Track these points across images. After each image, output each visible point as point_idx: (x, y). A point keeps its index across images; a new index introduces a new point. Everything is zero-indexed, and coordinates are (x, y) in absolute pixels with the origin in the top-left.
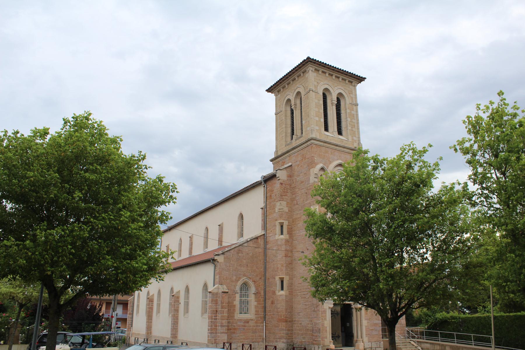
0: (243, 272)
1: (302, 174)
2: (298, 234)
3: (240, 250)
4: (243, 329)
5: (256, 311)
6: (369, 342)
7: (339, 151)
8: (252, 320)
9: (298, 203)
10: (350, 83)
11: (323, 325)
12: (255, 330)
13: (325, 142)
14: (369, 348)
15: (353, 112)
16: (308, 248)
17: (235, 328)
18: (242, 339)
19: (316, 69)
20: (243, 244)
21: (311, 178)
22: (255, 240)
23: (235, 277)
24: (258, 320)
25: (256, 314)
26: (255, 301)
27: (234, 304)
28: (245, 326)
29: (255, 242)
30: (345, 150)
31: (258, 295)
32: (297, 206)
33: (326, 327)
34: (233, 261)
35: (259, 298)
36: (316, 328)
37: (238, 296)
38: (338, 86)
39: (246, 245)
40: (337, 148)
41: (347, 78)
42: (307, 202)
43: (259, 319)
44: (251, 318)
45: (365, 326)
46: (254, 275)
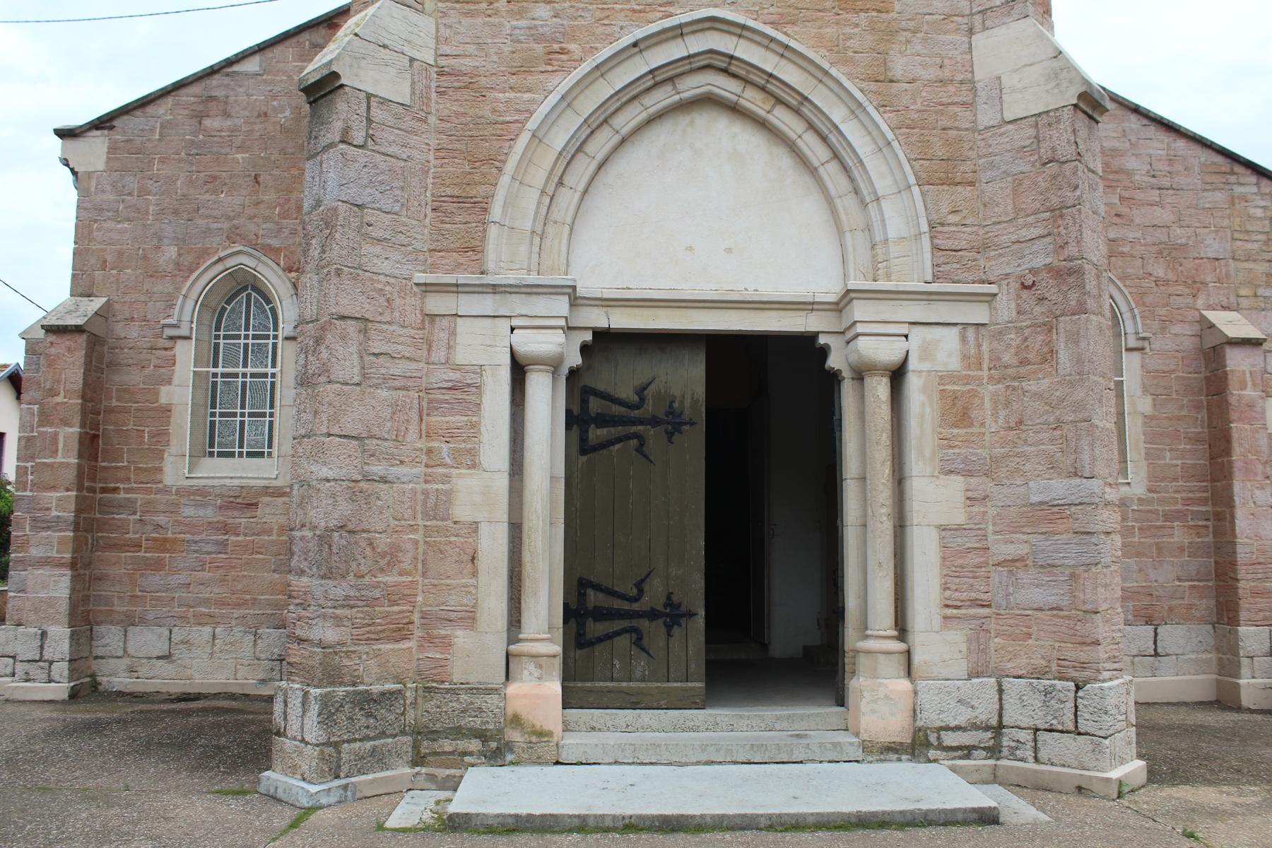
0: (229, 218)
4: (217, 543)
6: (972, 675)
14: (975, 727)
17: (166, 540)
18: (206, 602)
23: (171, 252)
28: (226, 529)
33: (474, 527)
34: (162, 161)
36: (309, 534)
39: (252, 65)
45: (942, 528)
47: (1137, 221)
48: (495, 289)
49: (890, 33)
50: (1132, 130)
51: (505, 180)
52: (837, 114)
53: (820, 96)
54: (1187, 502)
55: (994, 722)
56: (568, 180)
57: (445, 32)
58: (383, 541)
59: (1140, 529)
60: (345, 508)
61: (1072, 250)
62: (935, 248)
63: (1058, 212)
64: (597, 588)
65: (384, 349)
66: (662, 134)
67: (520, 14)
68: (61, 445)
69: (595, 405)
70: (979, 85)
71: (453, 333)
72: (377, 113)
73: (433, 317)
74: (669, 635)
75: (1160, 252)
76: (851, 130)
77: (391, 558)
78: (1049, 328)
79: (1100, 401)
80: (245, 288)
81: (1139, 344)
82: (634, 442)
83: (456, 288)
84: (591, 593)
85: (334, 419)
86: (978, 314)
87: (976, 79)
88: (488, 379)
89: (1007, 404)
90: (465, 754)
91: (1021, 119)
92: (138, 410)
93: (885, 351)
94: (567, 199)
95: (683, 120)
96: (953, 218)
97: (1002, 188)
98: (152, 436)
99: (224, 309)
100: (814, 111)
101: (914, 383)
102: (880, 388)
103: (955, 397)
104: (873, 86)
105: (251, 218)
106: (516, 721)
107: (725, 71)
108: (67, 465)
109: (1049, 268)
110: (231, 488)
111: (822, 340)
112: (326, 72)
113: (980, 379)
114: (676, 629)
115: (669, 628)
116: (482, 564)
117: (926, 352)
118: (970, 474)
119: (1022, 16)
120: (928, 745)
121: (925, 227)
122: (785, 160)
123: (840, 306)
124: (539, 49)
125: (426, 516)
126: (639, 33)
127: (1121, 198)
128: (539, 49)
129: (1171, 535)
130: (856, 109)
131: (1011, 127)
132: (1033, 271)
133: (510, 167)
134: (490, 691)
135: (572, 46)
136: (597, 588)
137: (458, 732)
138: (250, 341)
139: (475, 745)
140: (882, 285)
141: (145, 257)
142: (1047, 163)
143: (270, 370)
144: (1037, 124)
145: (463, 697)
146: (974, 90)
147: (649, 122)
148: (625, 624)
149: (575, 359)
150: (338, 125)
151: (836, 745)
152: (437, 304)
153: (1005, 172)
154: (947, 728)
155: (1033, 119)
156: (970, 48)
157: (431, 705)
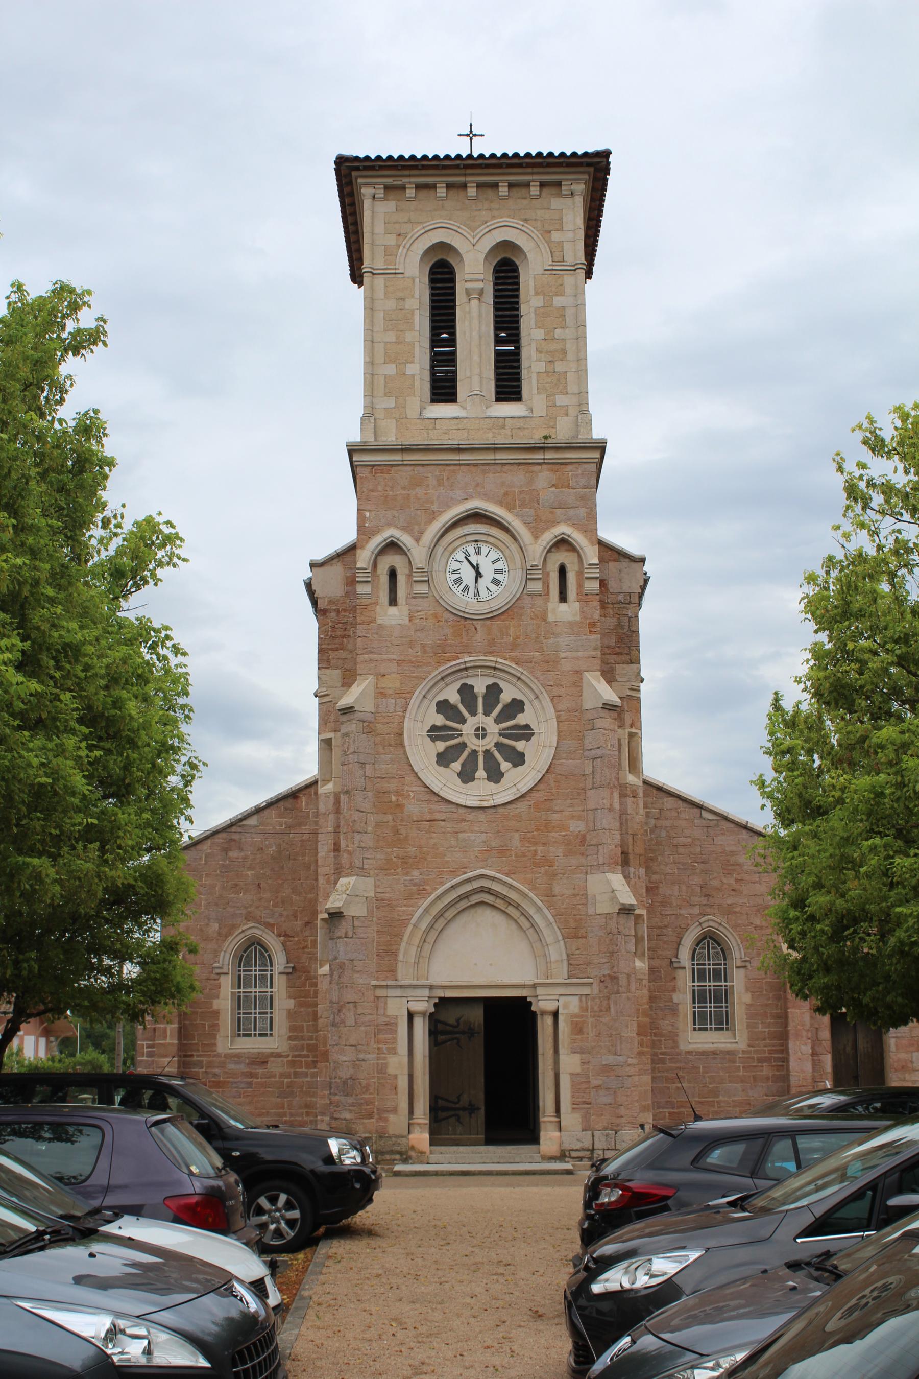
0: (246, 908)
3: (233, 840)
4: (247, 1083)
5: (292, 1028)
8: (279, 1055)
10: (554, 190)
11: (382, 1069)
12: (288, 1087)
13: (405, 450)
14: (583, 1150)
15: (558, 301)
17: (219, 1082)
19: (387, 188)
20: (241, 820)
22: (289, 803)
23: (216, 926)
24: (299, 1056)
25: (290, 1038)
26: (290, 997)
27: (215, 1007)
28: (251, 1075)
29: (286, 809)
30: (500, 456)
31: (300, 977)
33: (396, 1076)
34: (207, 875)
35: (304, 985)
36: (338, 1080)
37: (227, 985)
38: (493, 217)
39: (253, 821)
40: (465, 456)
41: (532, 173)
43: (305, 1052)
44: (276, 1051)
45: (572, 1074)
46: (285, 913)
47: (745, 893)
48: (401, 987)
49: (553, 876)
50: (743, 839)
51: (403, 945)
52: (531, 911)
53: (525, 904)
54: (770, 1052)
55: (591, 1148)
56: (428, 940)
57: (378, 883)
58: (364, 1082)
59: (744, 1067)
60: (351, 1071)
61: (615, 969)
62: (569, 964)
63: (612, 953)
64: (442, 1098)
65: (363, 1012)
66: (464, 918)
67: (407, 874)
68: (168, 1034)
69: (440, 1026)
71: (386, 1003)
72: (356, 923)
73: (378, 998)
74: (470, 1117)
75: (758, 911)
76: (537, 918)
77: (366, 1088)
78: (608, 998)
79: (627, 1026)
80: (253, 944)
81: (743, 964)
82: (455, 1041)
83: (387, 987)
84: (440, 1101)
85: (347, 1040)
86: (586, 990)
88: (399, 1020)
89: (596, 1026)
90: (395, 1160)
92: (202, 1013)
93: (550, 1006)
94: (427, 947)
95: (473, 911)
96: (578, 952)
98: (210, 1026)
99: (242, 956)
101: (561, 1018)
102: (549, 1020)
103: (577, 1023)
104: (546, 898)
105: (257, 907)
106: (413, 1148)
107: (488, 893)
108: (172, 1044)
109: (609, 975)
110: (253, 1054)
111: (529, 999)
113: (587, 1016)
114: (473, 1115)
115: (470, 1114)
116: (399, 1090)
117: (566, 1006)
118: (582, 1053)
120: (565, 1156)
121: (565, 957)
122: (514, 926)
123: (534, 986)
124: (415, 889)
125: (378, 1073)
126: (454, 882)
127: (736, 880)
128: (415, 889)
129: (762, 1071)
130: (539, 909)
132: (604, 976)
133: (405, 938)
134: (403, 1137)
135: (427, 887)
136: (442, 1098)
137: (392, 1152)
138: (258, 973)
139: (398, 1157)
140: (550, 981)
141: (201, 930)
143: (269, 990)
145: (393, 1139)
146: (587, 898)
147: (459, 913)
148: (453, 1113)
149: (432, 1010)
150: (344, 931)
151: (531, 1157)
152: (380, 993)
154: (573, 1150)
157: (381, 1143)
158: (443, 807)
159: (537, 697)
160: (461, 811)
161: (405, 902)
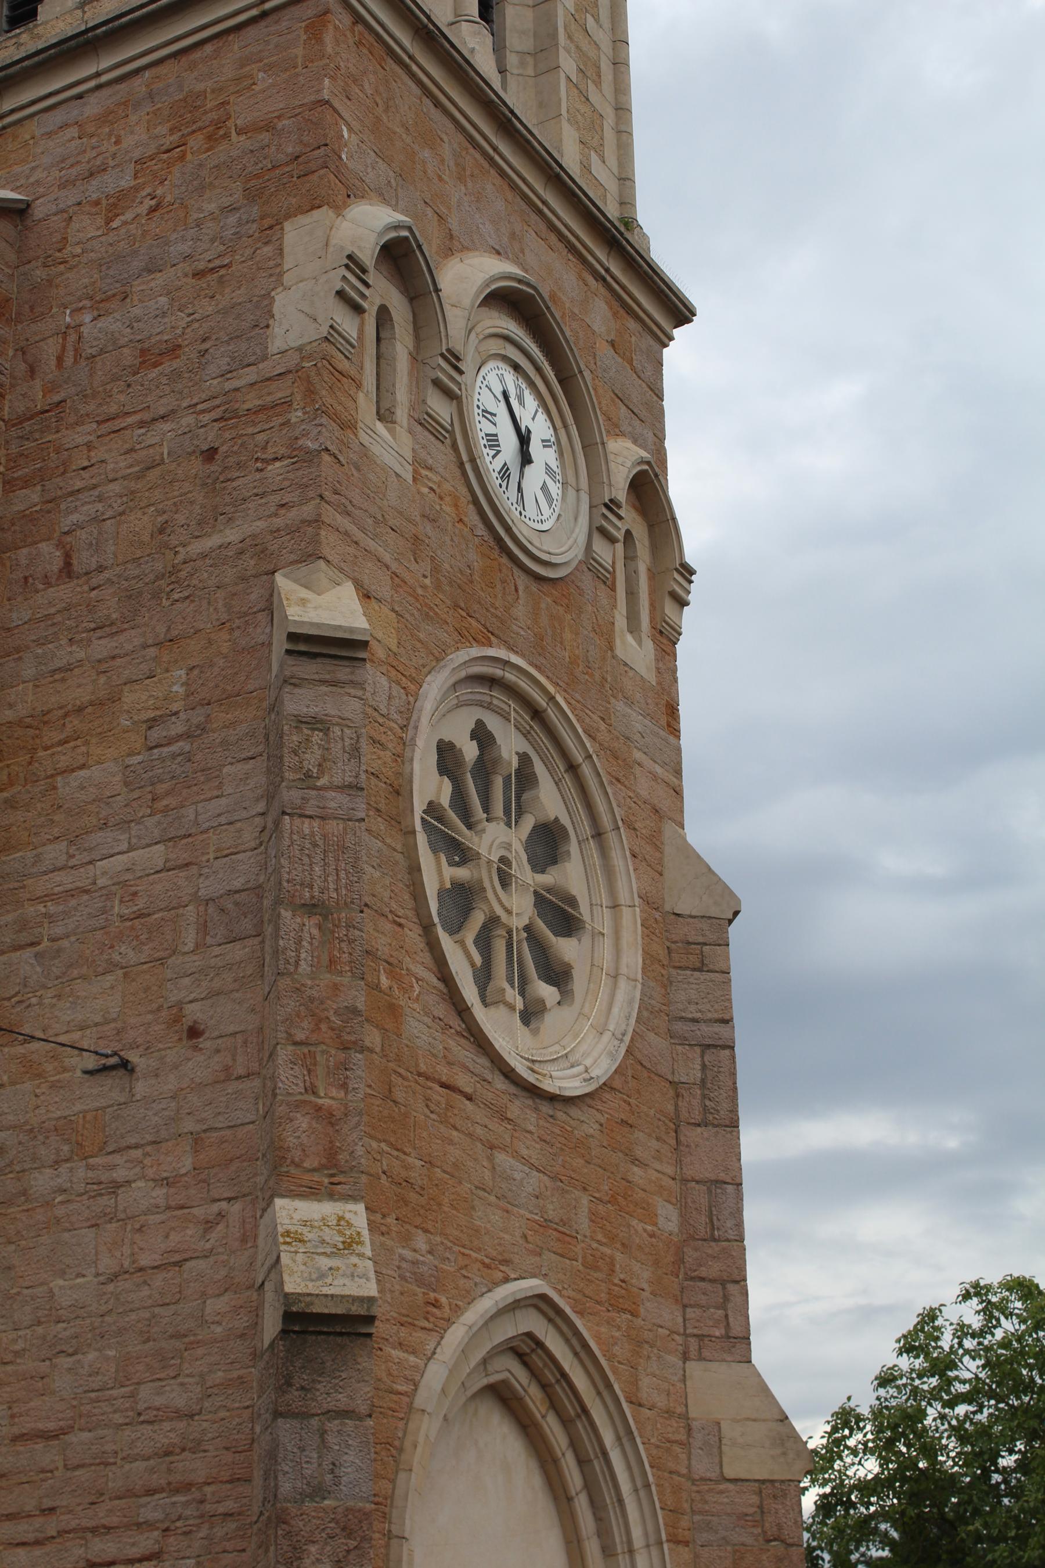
1: (159, 280)
2: (65, 880)
7: (513, 187)
9: (83, 560)
16: (194, 1012)
21: (285, 304)
32: (64, 593)
42: (215, 541)
70: (695, 1425)
87: (691, 1415)
91: (743, 1480)
97: (720, 1557)
100: (589, 1429)
112: (356, 1309)
119: (744, 1359)
131: (730, 1486)
135: (443, 1300)
142: (771, 1541)
144: (761, 1492)
146: (689, 1430)
153: (724, 1538)
155: (757, 1485)
156: (684, 1376)
158: (464, 1052)
159: (598, 835)
160: (500, 1083)
161: (403, 1332)
